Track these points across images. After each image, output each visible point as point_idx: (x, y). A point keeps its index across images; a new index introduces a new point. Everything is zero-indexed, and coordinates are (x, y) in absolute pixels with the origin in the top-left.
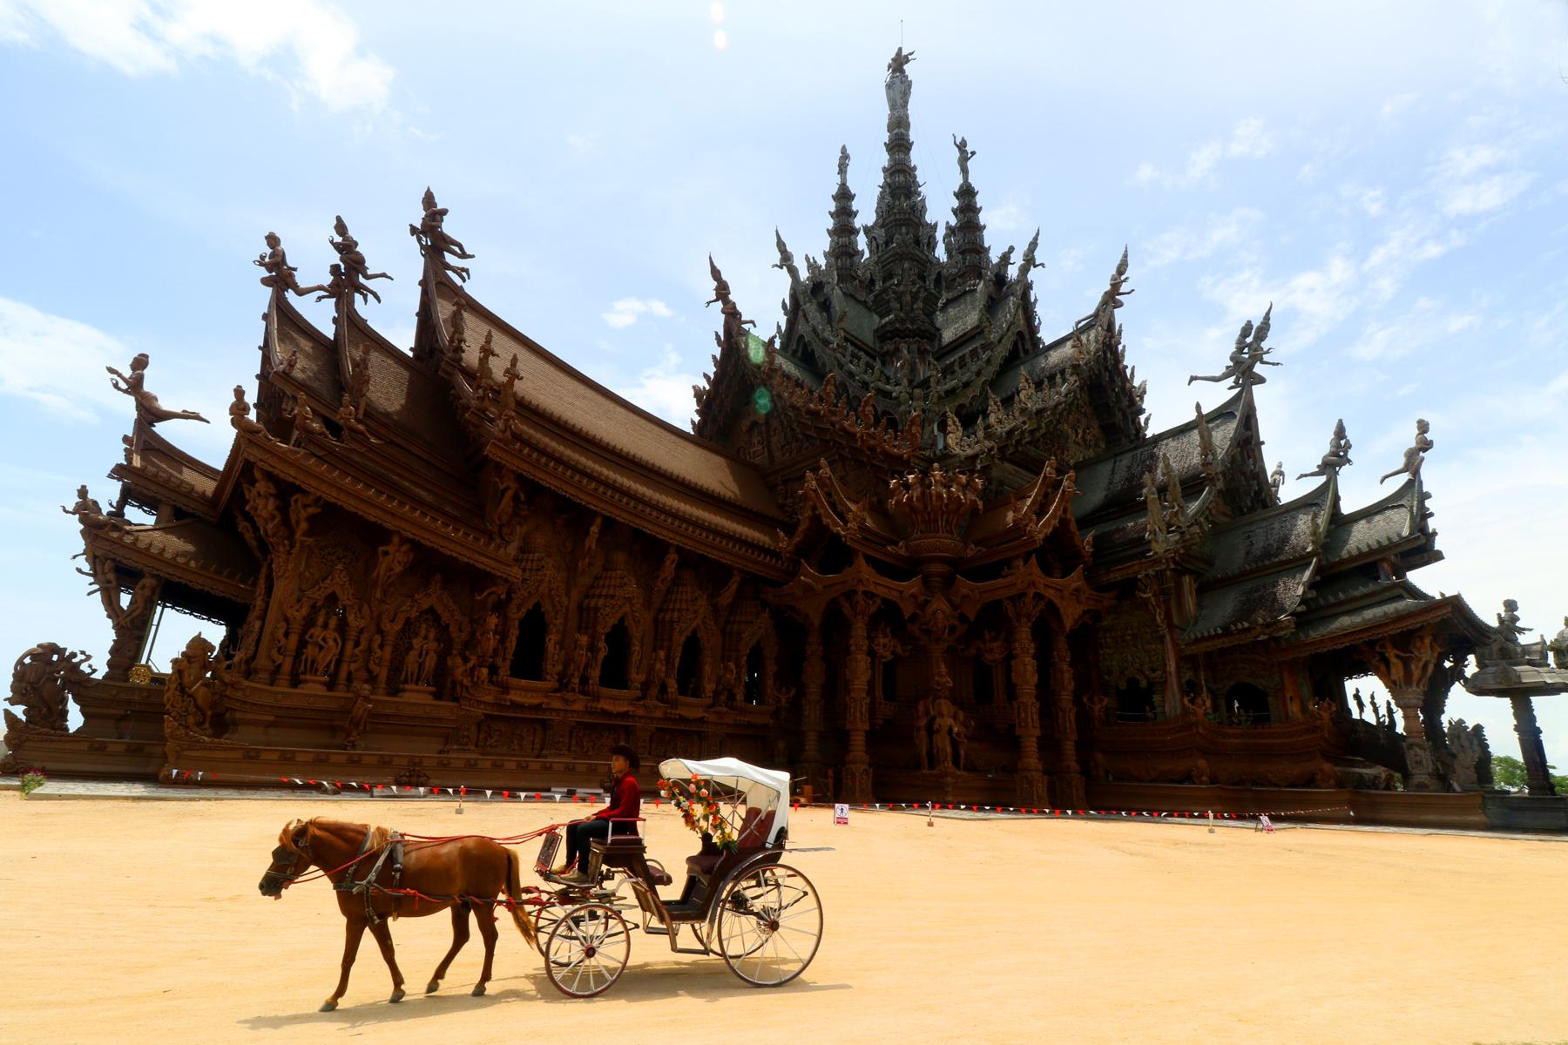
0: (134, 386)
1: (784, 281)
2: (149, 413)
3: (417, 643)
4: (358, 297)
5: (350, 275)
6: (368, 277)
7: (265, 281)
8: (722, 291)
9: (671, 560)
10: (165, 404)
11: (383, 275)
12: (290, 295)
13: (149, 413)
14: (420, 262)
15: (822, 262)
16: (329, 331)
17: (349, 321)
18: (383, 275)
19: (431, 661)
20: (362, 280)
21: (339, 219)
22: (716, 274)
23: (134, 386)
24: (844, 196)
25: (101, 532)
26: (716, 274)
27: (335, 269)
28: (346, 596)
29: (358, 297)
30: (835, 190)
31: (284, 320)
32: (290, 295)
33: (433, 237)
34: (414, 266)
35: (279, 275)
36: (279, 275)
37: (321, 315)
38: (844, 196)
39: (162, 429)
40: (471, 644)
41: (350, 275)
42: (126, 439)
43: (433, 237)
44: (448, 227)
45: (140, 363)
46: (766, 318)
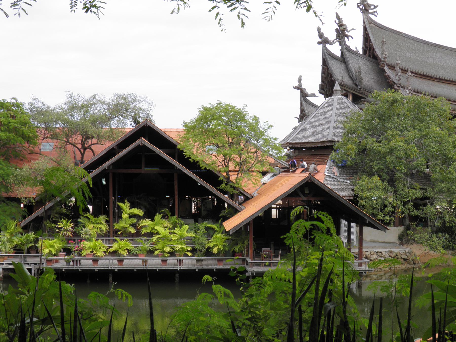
0: (299, 88)
2: (304, 95)
4: (346, 38)
5: (342, 33)
6: (348, 32)
10: (309, 92)
11: (353, 29)
12: (328, 46)
13: (304, 95)
17: (345, 49)
18: (353, 29)
20: (346, 33)
21: (337, 14)
23: (299, 88)
27: (337, 30)
35: (324, 41)
37: (336, 49)
41: (342, 33)
45: (300, 80)
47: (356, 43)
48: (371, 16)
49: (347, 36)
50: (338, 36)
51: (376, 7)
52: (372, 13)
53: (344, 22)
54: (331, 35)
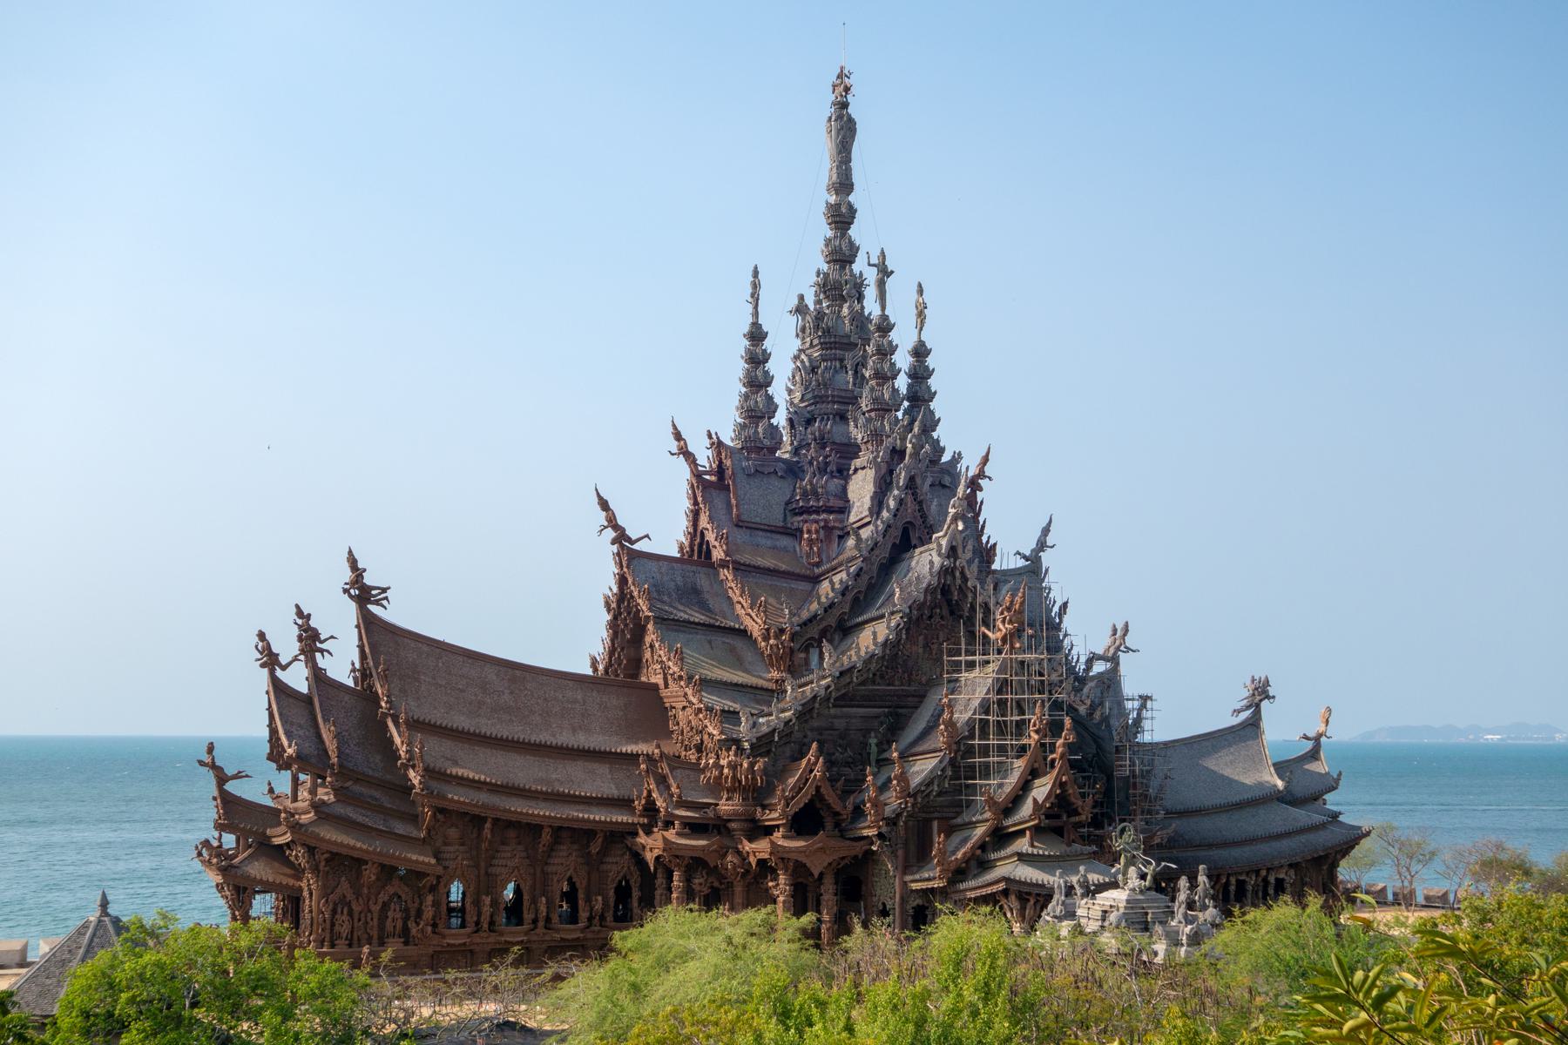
0: (213, 766)
1: (683, 471)
2: (222, 779)
3: (390, 914)
4: (318, 655)
5: (310, 640)
7: (263, 666)
8: (612, 522)
9: (546, 837)
10: (230, 771)
14: (352, 607)
15: (728, 437)
16: (303, 688)
17: (318, 676)
19: (399, 924)
21: (297, 606)
22: (604, 505)
23: (213, 766)
24: (757, 335)
25: (212, 854)
26: (604, 505)
27: (300, 639)
28: (350, 896)
29: (318, 655)
30: (746, 329)
31: (280, 690)
32: (279, 673)
33: (363, 594)
34: (349, 611)
35: (270, 660)
36: (270, 660)
37: (297, 678)
38: (757, 335)
39: (230, 787)
40: (419, 914)
41: (310, 640)
42: (215, 799)
43: (363, 594)
44: (368, 580)
46: (664, 528)
47: (341, 663)
48: (371, 607)
49: (322, 651)
50: (302, 651)
51: (384, 590)
52: (377, 603)
53: (313, 623)
54: (287, 645)
